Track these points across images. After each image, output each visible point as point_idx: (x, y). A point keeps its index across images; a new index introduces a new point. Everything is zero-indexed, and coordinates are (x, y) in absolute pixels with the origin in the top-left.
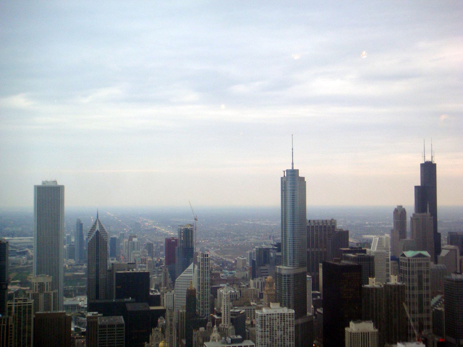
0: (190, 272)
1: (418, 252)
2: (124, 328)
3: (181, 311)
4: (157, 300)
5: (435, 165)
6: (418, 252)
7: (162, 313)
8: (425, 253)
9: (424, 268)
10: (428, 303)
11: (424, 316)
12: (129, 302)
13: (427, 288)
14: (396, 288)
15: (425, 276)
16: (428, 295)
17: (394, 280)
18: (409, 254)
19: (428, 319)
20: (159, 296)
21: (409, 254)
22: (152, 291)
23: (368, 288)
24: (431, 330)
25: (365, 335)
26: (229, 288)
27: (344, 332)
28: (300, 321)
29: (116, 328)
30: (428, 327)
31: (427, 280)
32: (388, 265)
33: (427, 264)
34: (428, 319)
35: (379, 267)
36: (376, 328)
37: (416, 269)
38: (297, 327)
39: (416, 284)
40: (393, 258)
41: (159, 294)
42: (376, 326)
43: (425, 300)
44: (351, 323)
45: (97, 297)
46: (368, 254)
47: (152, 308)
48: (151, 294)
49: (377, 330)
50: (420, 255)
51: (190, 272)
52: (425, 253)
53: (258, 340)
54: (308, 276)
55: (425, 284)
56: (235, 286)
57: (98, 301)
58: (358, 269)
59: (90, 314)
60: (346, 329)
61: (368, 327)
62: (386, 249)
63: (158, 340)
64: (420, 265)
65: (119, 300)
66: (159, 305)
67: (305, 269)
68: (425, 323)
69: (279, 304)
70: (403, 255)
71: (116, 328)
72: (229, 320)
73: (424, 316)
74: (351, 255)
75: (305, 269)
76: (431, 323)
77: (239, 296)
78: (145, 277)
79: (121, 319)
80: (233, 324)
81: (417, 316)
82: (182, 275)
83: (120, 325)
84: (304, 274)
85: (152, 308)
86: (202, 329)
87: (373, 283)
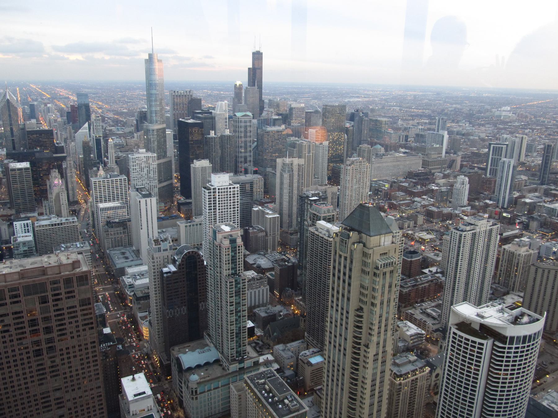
0: (86, 129)
1: (244, 113)
2: (30, 170)
3: (81, 156)
4: (60, 150)
5: (262, 54)
6: (244, 113)
7: (64, 158)
9: (248, 124)
10: (250, 146)
11: (248, 154)
12: (38, 152)
13: (250, 137)
14: (229, 137)
15: (249, 129)
16: (250, 141)
17: (227, 132)
19: (250, 156)
20: (63, 146)
21: (239, 114)
22: (57, 143)
24: (252, 163)
25: (203, 169)
26: (118, 139)
27: (189, 167)
28: (162, 161)
29: (24, 171)
30: (250, 161)
31: (250, 132)
32: (226, 122)
33: (250, 121)
34: (250, 156)
35: (220, 124)
36: (212, 163)
37: (243, 124)
38: (159, 165)
39: (243, 135)
40: (230, 117)
41: (63, 145)
42: (211, 162)
43: (248, 144)
44: (195, 161)
45: (14, 148)
46: (213, 115)
47: (55, 155)
48: (57, 145)
49: (211, 165)
50: (245, 115)
51: (86, 129)
52: (249, 114)
53: (132, 175)
54: (167, 130)
55: (248, 134)
56: (122, 138)
57: (13, 152)
58: (200, 126)
59: (6, 162)
60: (192, 165)
61: (205, 163)
62: (225, 111)
63: (56, 177)
64: (245, 122)
65: (30, 151)
66: (64, 153)
68: (248, 159)
69: (145, 150)
70: (235, 115)
71: (24, 171)
72: (114, 162)
73: (248, 154)
74: (200, 115)
76: (252, 159)
77: (125, 144)
78: (49, 133)
79: (25, 165)
80: (117, 164)
81: (243, 155)
82: (80, 131)
83: (26, 169)
84: (164, 130)
85: (55, 155)
86: (95, 169)
87: (212, 134)
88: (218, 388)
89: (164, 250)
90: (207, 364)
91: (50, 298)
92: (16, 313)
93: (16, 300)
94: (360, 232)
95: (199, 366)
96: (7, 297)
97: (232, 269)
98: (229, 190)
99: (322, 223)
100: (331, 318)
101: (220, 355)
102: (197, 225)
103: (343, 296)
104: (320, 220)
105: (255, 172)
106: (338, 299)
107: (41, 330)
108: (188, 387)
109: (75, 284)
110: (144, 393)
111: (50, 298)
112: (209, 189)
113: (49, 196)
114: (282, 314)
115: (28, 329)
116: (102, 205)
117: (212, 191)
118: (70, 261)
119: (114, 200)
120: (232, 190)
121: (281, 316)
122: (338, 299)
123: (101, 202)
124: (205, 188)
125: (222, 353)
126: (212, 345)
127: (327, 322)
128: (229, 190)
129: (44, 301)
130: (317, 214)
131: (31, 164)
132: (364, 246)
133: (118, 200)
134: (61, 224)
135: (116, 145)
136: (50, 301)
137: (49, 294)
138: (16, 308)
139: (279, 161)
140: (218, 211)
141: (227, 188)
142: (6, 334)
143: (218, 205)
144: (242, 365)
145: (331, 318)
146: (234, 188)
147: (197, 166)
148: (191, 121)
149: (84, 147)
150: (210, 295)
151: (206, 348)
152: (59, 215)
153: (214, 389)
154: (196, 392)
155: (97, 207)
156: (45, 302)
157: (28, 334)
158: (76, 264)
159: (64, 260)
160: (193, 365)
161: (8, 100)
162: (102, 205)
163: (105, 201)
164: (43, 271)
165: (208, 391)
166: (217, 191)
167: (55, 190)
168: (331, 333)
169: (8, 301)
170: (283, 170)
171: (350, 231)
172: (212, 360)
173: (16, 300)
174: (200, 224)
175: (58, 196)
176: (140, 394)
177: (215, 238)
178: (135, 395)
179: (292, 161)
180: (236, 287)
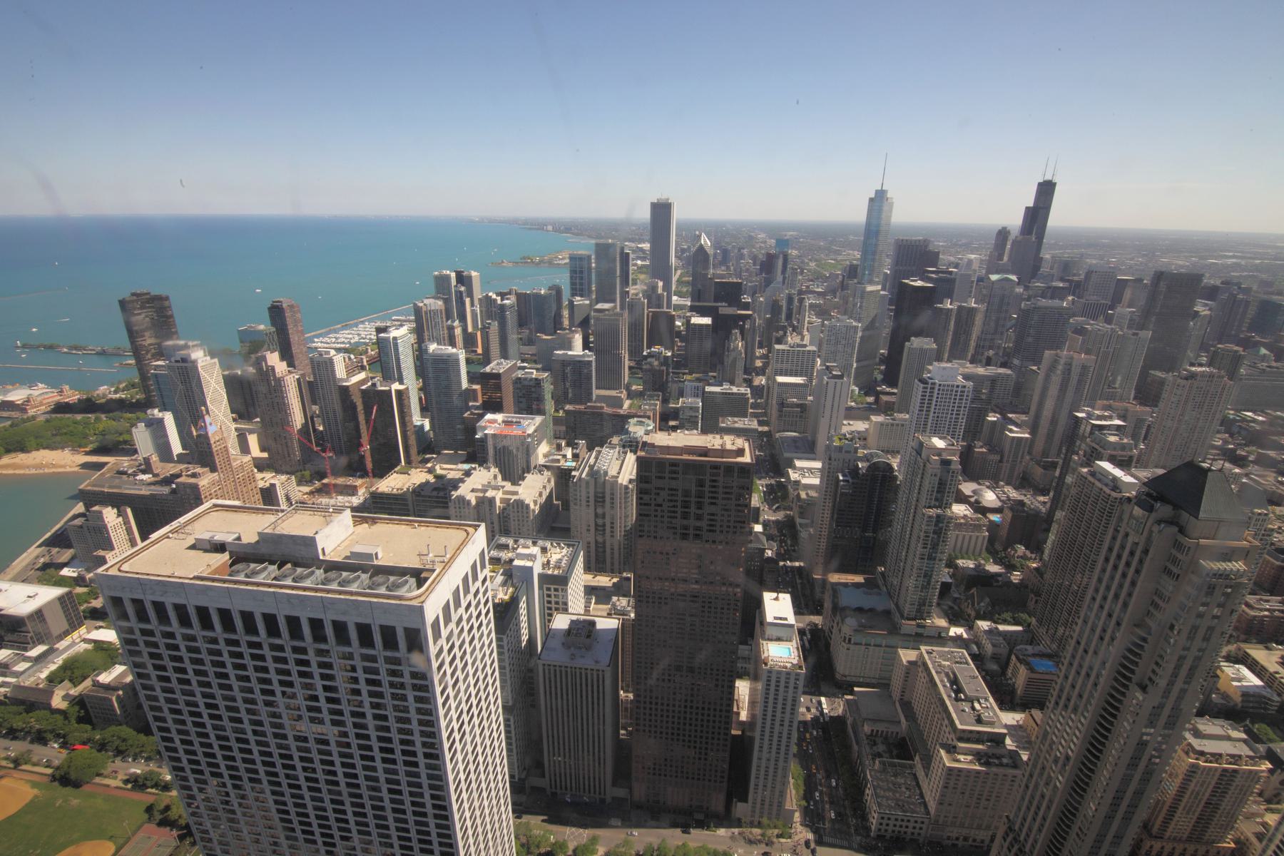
4: (746, 306)
5: (1054, 184)
8: (1014, 278)
10: (1003, 326)
18: (994, 277)
21: (994, 277)
23: (941, 309)
25: (923, 352)
27: (902, 347)
28: (867, 333)
52: (1014, 278)
59: (688, 314)
67: (879, 287)
75: (879, 287)
79: (707, 321)
83: (707, 325)
86: (781, 333)
88: (880, 646)
89: (847, 452)
90: (871, 610)
91: (708, 483)
92: (672, 490)
93: (674, 476)
94: (1176, 507)
95: (860, 610)
96: (667, 471)
97: (936, 499)
98: (955, 389)
99: (1106, 465)
100: (1085, 622)
101: (893, 606)
102: (898, 425)
103: (1116, 596)
104: (1101, 460)
105: (1004, 365)
106: (1105, 598)
107: (692, 514)
108: (840, 630)
109: (736, 474)
110: (786, 619)
111: (708, 483)
112: (927, 383)
113: (726, 359)
114: (1000, 579)
115: (679, 510)
116: (780, 379)
117: (929, 386)
118: (734, 448)
119: (796, 375)
120: (960, 389)
121: (998, 581)
122: (1105, 598)
123: (781, 375)
124: (920, 381)
125: (897, 605)
126: (885, 589)
127: (1077, 624)
128: (955, 389)
129: (701, 484)
130: (1100, 449)
131: (713, 321)
132: (1182, 531)
133: (801, 376)
134: (733, 394)
135: (811, 306)
136: (707, 486)
137: (707, 478)
138: (674, 484)
139: (1047, 352)
140: (931, 414)
141: (953, 386)
142: (659, 508)
143: (933, 407)
144: (920, 631)
145: (1085, 622)
146: (964, 387)
147: (915, 345)
148: (919, 283)
149: (773, 305)
150: (897, 527)
151: (876, 590)
152: (732, 383)
153: (875, 645)
154: (850, 640)
155: (775, 380)
156: (702, 486)
157: (679, 515)
158: (740, 452)
159: (729, 447)
160: (855, 604)
161: (701, 245)
162: (780, 379)
163: (786, 375)
164: (705, 452)
165: (866, 645)
166: (937, 387)
167: (733, 355)
168: (1078, 643)
169: (667, 475)
170: (1052, 368)
171: (1156, 499)
172: (880, 608)
173: (674, 476)
174: (903, 425)
175: (735, 360)
176: (780, 619)
177: (919, 453)
178: (776, 618)
179: (1072, 358)
180: (936, 525)
